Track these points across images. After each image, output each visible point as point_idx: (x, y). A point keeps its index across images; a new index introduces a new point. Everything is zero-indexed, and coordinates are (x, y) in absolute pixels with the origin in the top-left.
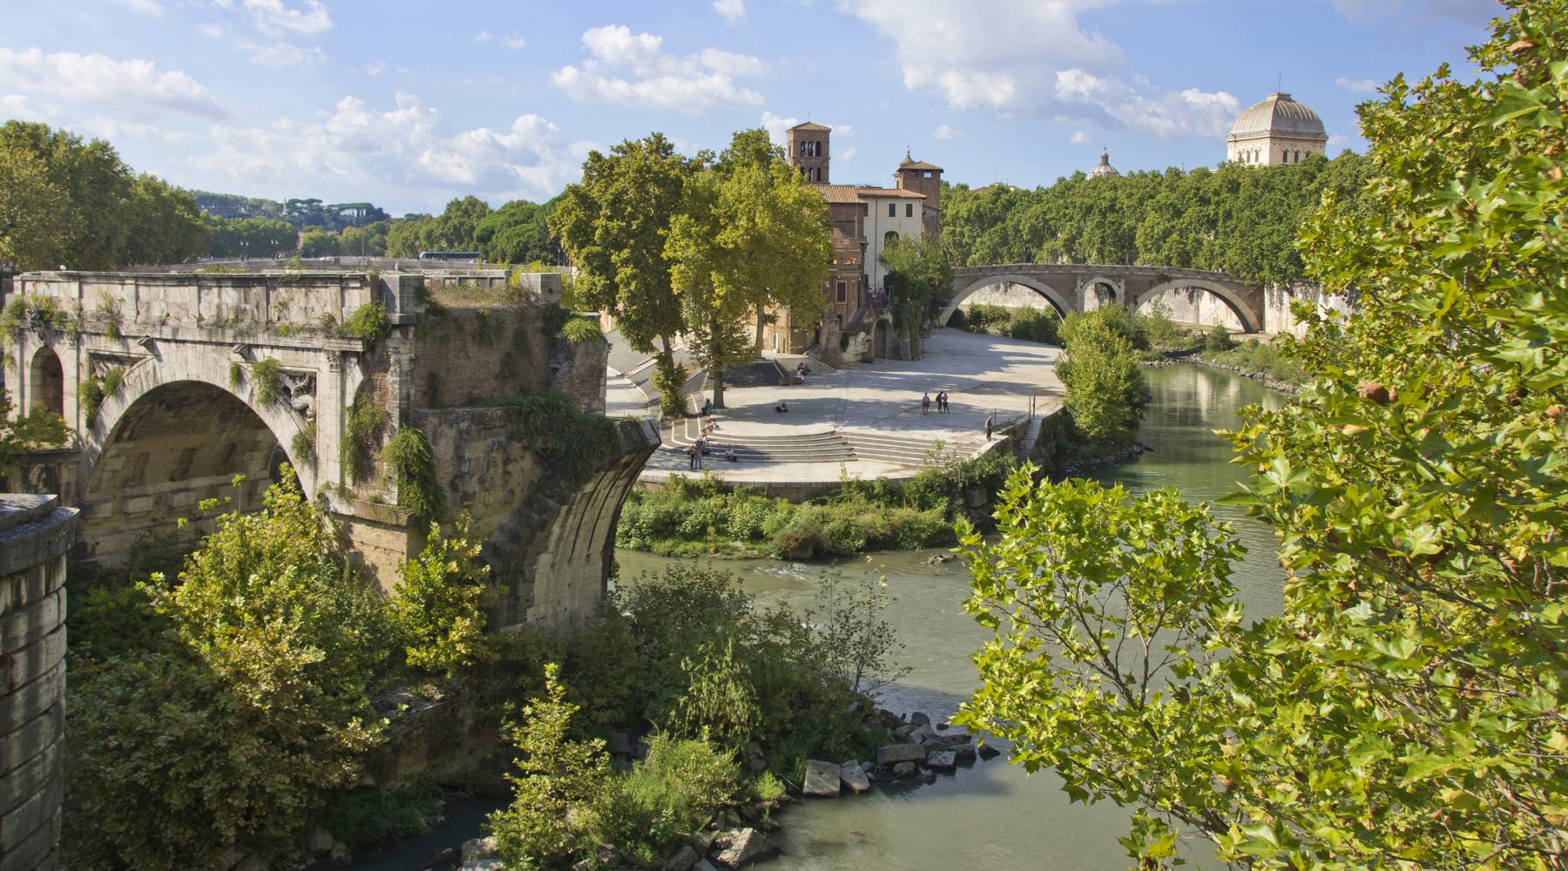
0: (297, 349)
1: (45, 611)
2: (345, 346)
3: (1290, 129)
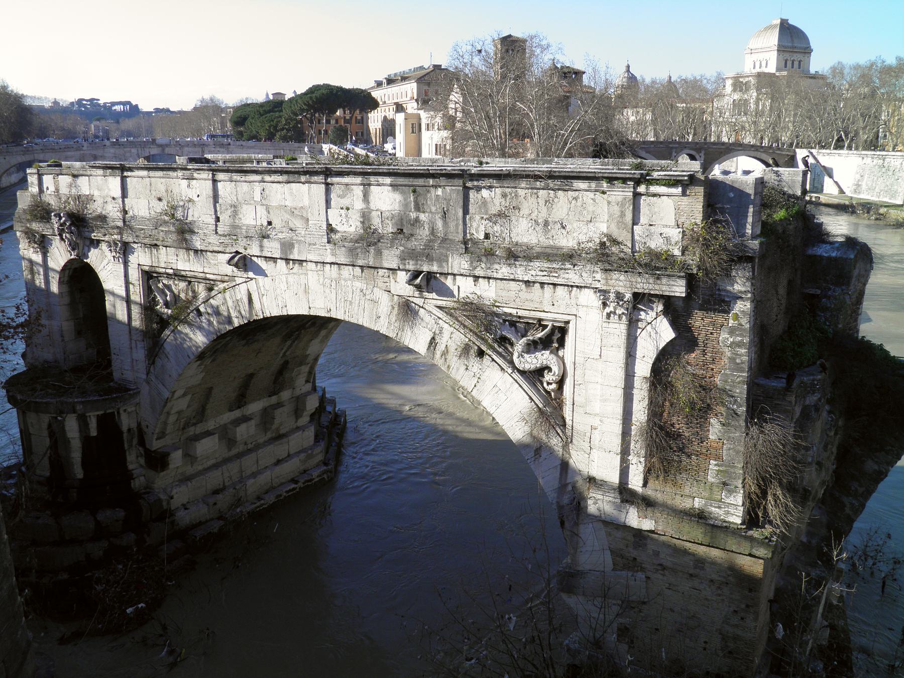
0: (527, 283)
2: (645, 284)
3: (790, 44)
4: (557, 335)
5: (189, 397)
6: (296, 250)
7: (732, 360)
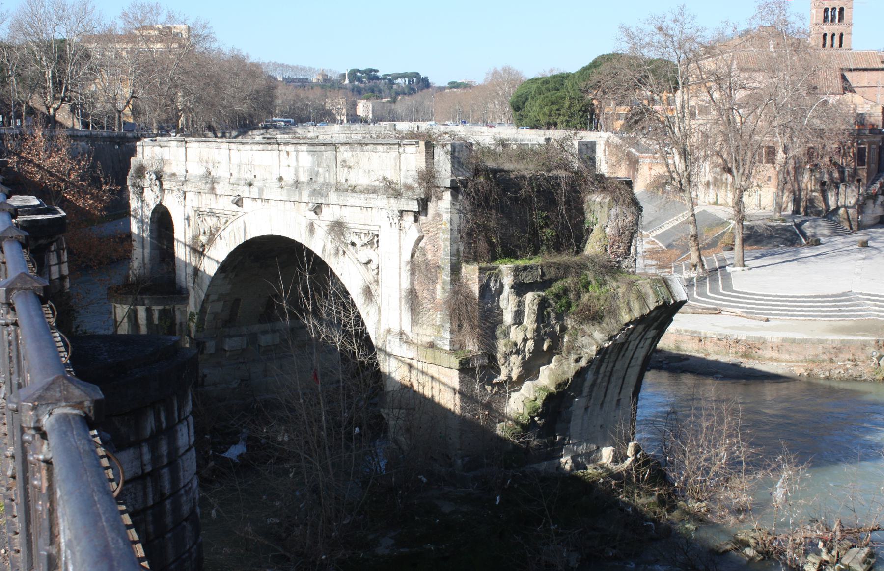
1: (179, 434)
4: (376, 239)
5: (222, 303)
6: (265, 193)
7: (444, 249)
